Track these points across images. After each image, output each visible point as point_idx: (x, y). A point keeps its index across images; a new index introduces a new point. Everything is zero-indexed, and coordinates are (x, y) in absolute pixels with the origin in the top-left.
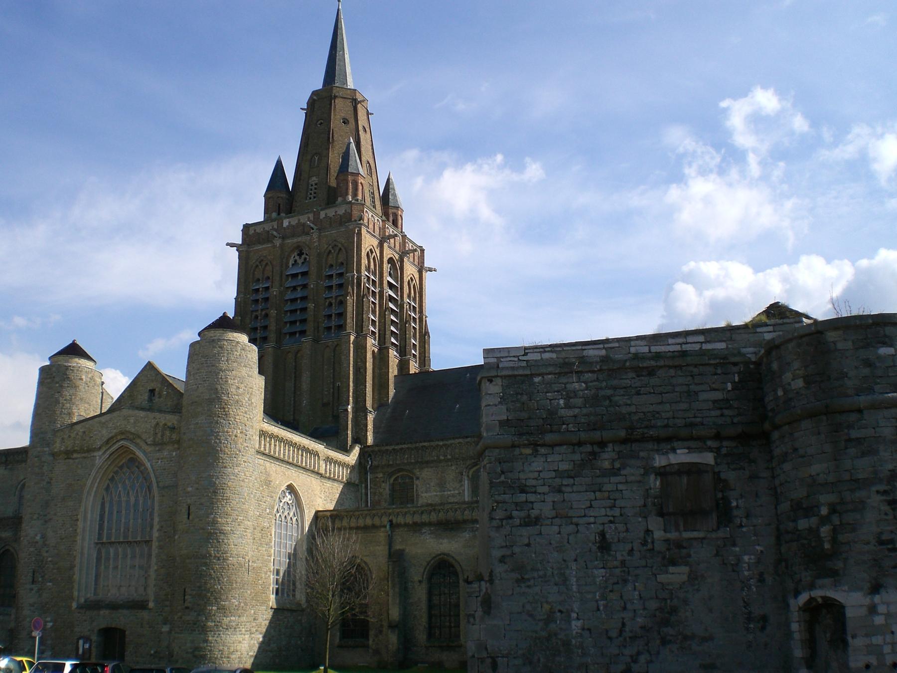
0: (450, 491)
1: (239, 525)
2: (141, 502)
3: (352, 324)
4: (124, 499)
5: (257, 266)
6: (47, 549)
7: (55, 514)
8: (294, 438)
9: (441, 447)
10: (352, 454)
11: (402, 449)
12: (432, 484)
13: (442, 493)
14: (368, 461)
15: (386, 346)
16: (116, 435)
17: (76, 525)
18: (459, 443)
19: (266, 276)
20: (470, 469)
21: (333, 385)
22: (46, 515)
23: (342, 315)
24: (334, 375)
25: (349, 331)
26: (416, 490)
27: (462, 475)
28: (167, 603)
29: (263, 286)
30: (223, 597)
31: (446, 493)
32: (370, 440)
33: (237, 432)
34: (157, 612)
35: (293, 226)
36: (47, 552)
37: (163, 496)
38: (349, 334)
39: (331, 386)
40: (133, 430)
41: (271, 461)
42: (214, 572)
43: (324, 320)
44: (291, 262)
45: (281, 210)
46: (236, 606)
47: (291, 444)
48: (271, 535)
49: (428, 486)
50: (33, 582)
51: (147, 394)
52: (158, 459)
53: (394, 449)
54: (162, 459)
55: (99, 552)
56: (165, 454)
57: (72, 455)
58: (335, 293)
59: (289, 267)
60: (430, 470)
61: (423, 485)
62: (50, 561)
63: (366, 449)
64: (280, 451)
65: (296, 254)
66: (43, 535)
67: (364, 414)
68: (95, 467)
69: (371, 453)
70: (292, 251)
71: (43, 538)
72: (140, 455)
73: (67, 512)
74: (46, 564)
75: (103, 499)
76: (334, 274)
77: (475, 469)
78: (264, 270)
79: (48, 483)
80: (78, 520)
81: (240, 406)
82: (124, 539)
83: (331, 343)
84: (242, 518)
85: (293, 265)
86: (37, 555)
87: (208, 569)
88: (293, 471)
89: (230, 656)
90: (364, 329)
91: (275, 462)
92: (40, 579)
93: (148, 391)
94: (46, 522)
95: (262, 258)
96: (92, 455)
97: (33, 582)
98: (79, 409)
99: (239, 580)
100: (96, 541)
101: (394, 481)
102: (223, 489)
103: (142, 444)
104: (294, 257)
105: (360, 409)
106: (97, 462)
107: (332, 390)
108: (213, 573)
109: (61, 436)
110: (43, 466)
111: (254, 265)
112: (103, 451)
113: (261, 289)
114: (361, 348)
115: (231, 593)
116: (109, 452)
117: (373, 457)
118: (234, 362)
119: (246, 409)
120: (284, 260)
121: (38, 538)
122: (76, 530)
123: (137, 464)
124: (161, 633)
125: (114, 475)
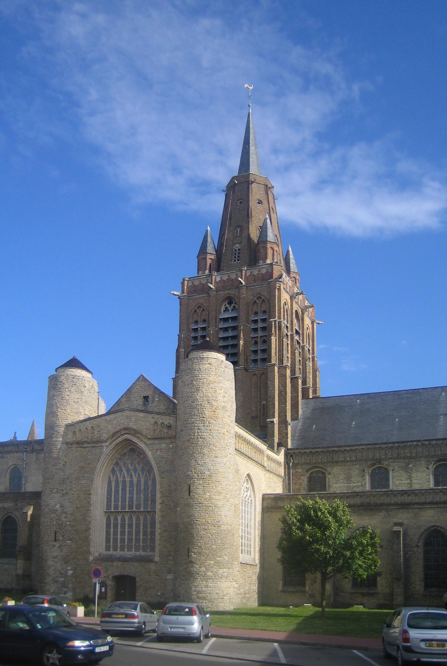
0: (355, 483)
1: (228, 501)
2: (142, 482)
3: (275, 358)
4: (128, 479)
5: (196, 311)
7: (71, 490)
8: (251, 439)
9: (348, 451)
10: (281, 454)
11: (317, 452)
12: (341, 478)
13: (348, 485)
14: (290, 461)
15: (296, 376)
17: (90, 498)
18: (362, 449)
19: (203, 319)
20: (371, 467)
21: (260, 403)
22: (63, 490)
23: (267, 351)
24: (260, 396)
25: (273, 363)
26: (329, 482)
27: (365, 472)
29: (201, 327)
30: (219, 554)
31: (351, 485)
32: (290, 446)
33: (224, 431)
35: (224, 281)
37: (163, 478)
38: (274, 365)
39: (259, 404)
40: (135, 427)
41: (239, 455)
42: (212, 535)
43: (252, 354)
44: (223, 308)
45: (212, 269)
46: (227, 561)
47: (249, 443)
48: (240, 510)
49: (337, 479)
50: (55, 540)
51: (141, 400)
52: (157, 450)
53: (311, 452)
54: (161, 449)
55: (108, 519)
57: (83, 444)
58: (260, 334)
59: (221, 312)
60: (338, 467)
61: (333, 478)
63: (289, 451)
64: (244, 448)
65: (227, 303)
66: (61, 505)
67: (285, 426)
68: (103, 455)
69: (293, 454)
70: (224, 300)
71: (63, 507)
72: (142, 446)
73: (81, 488)
74: (65, 527)
75: (110, 478)
76: (259, 319)
77: (373, 468)
78: (201, 314)
79: (64, 465)
80: (90, 494)
81: (226, 411)
82: (136, 509)
83: (258, 371)
84: (229, 496)
85: (224, 311)
86: (57, 520)
87: (207, 533)
88: (251, 464)
89: (224, 597)
90: (284, 362)
91: (241, 456)
93: (142, 397)
94: (63, 495)
95: (199, 305)
96: (100, 445)
97: (55, 540)
98: (84, 410)
99: (228, 542)
101: (310, 475)
102: (216, 474)
103: (142, 438)
104: (225, 305)
105: (283, 422)
106: (104, 450)
107: (259, 407)
108: (211, 536)
109: (72, 430)
111: (193, 310)
113: (199, 329)
114: (283, 377)
115: (223, 551)
116: (114, 443)
117: (294, 457)
118: (220, 376)
119: (230, 414)
120: (218, 307)
121: (58, 506)
122: (90, 502)
123: (137, 453)
124: (166, 580)
125: (118, 460)
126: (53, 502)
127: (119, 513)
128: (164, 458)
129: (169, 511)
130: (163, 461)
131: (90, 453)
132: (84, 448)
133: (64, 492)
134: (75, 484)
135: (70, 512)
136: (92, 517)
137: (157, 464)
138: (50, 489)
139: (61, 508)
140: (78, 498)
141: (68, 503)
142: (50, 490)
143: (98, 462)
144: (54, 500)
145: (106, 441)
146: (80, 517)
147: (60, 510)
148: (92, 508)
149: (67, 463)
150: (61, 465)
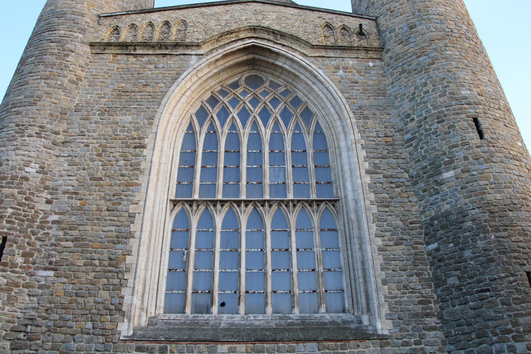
6: (49, 197)
7: (82, 134)
16: (239, 30)
28: (432, 321)
34: (406, 344)
36: (48, 202)
37: (366, 118)
52: (337, 68)
56: (351, 63)
57: (135, 49)
62: (54, 222)
66: (42, 168)
71: (46, 173)
79: (72, 82)
92: (19, 260)
100: (173, 198)
106: (192, 62)
110: (67, 55)
112: (207, 50)
121: (32, 170)
122: (138, 164)
126: (19, 158)
127: (219, 206)
128: (357, 83)
129: (398, 190)
130: (355, 88)
131: (152, 67)
132: (136, 55)
133: (61, 138)
134: (96, 123)
135: (71, 188)
136: (142, 203)
137: (343, 92)
138: (18, 125)
139: (41, 175)
140: (99, 155)
141: (66, 165)
142: (17, 128)
143: (173, 83)
144: (26, 153)
145: (198, 46)
146: (102, 202)
147: (35, 179)
148: (142, 179)
149: (81, 81)
150: (67, 81)
